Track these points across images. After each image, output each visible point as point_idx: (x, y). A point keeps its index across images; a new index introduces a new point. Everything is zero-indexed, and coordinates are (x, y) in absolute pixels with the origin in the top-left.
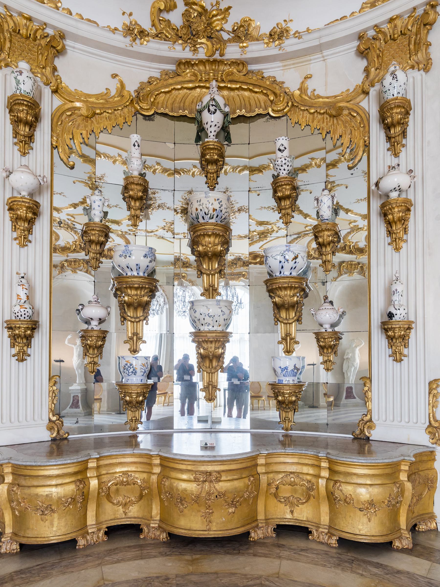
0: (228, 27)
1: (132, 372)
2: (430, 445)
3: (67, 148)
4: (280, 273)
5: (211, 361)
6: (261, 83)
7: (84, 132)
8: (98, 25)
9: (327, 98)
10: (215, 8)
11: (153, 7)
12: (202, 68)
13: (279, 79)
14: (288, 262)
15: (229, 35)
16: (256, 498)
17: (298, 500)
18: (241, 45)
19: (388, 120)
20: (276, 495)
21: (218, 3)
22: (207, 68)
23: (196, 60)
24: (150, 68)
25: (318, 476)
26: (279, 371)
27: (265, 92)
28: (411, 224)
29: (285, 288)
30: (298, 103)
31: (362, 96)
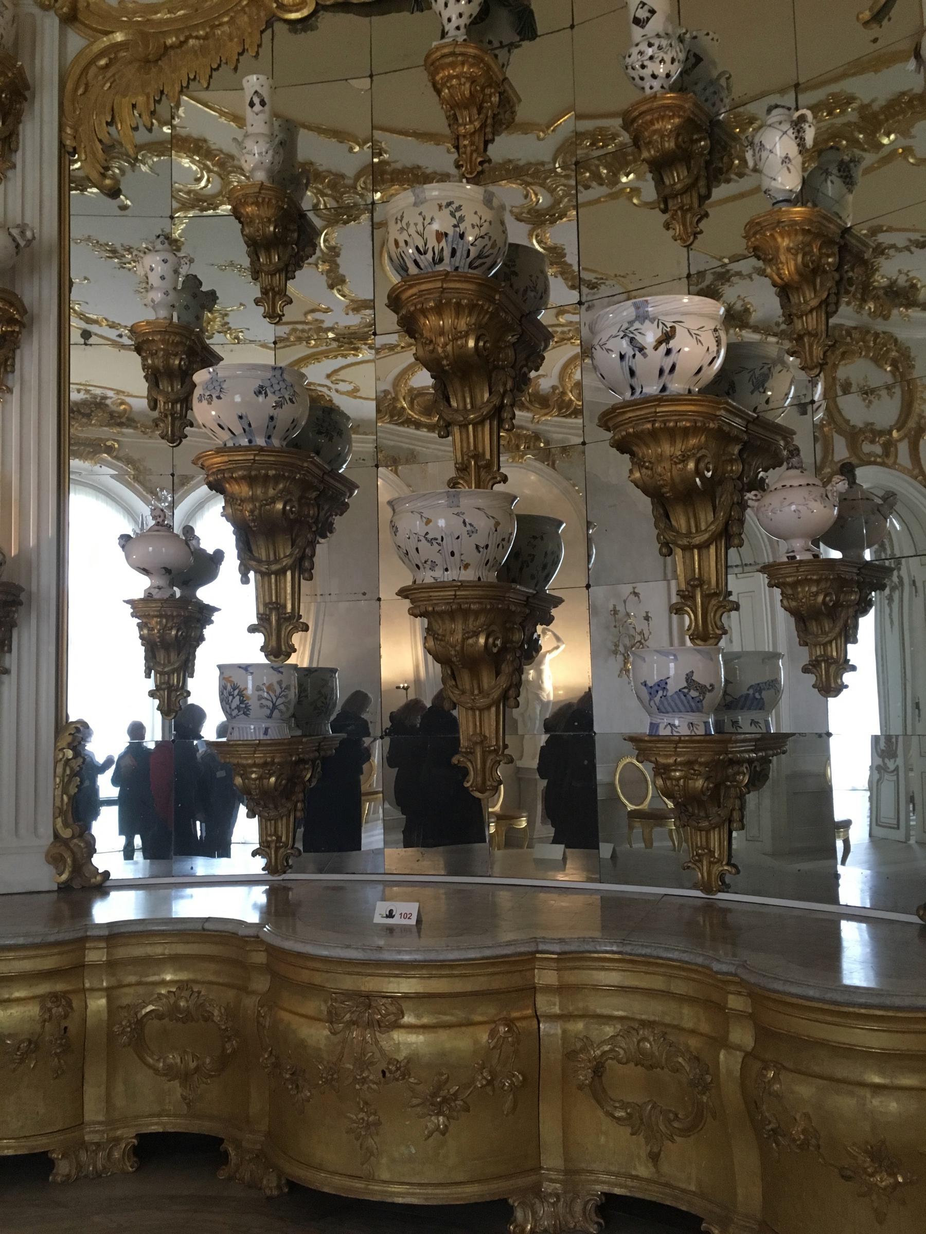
1: (238, 708)
3: (99, 147)
4: (633, 389)
7: (140, 100)
14: (645, 355)
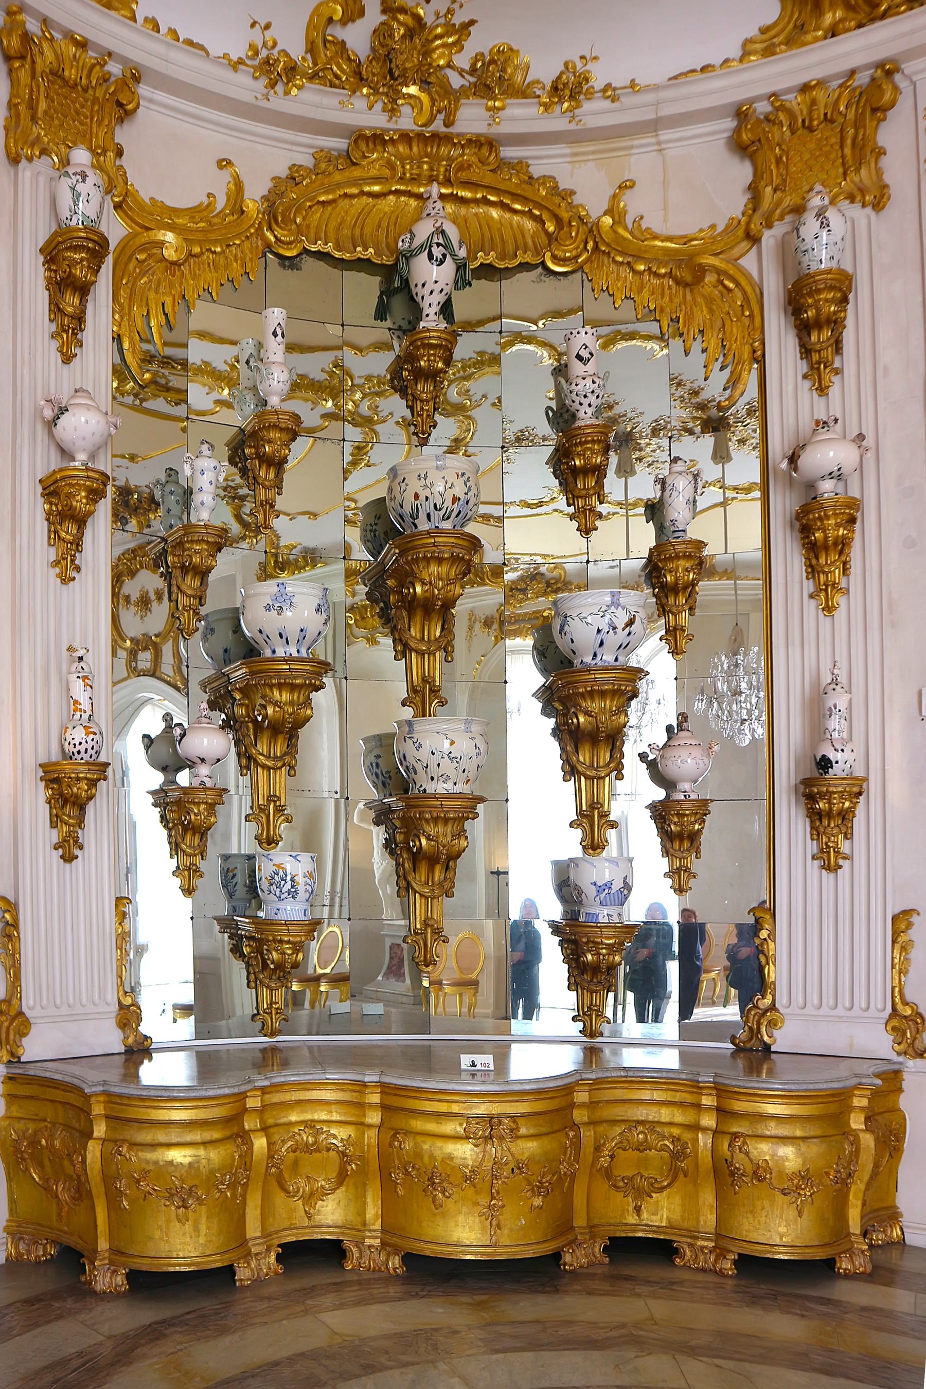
0: (463, 60)
3: (138, 338)
4: (595, 655)
6: (527, 192)
7: (168, 301)
8: (208, 54)
9: (670, 239)
10: (442, 20)
11: (316, 11)
12: (402, 148)
13: (564, 184)
14: (615, 633)
15: (463, 77)
18: (490, 103)
19: (810, 313)
21: (450, 11)
22: (415, 149)
23: (395, 131)
24: (293, 143)
27: (537, 212)
29: (603, 694)
30: (608, 245)
31: (745, 245)
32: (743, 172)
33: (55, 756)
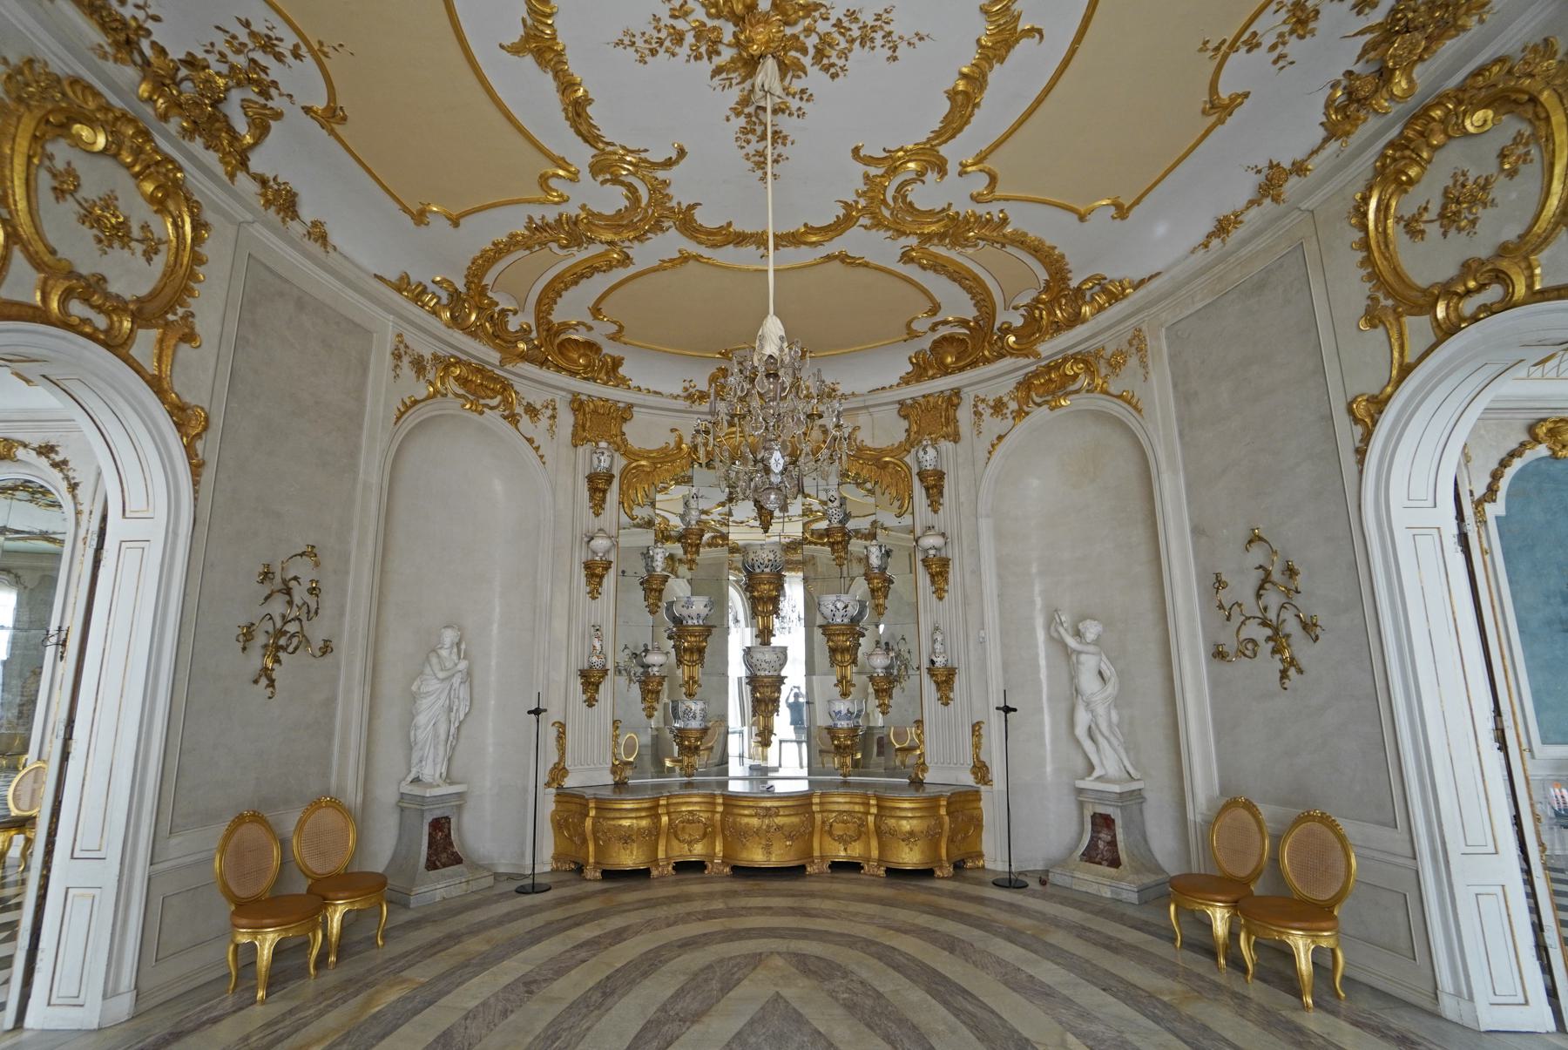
2: (974, 784)
5: (767, 705)
7: (646, 486)
16: (811, 834)
17: (850, 837)
20: (830, 833)
25: (867, 813)
26: (833, 715)
28: (951, 577)
29: (838, 635)
32: (905, 424)
33: (586, 667)
